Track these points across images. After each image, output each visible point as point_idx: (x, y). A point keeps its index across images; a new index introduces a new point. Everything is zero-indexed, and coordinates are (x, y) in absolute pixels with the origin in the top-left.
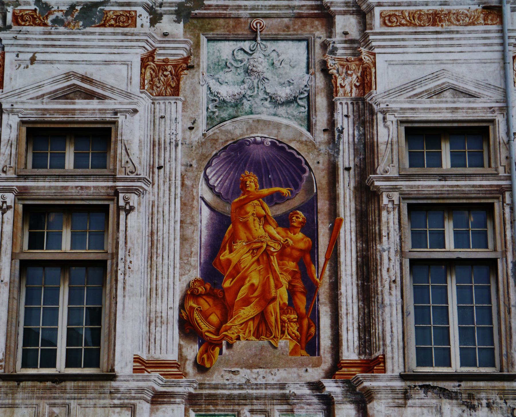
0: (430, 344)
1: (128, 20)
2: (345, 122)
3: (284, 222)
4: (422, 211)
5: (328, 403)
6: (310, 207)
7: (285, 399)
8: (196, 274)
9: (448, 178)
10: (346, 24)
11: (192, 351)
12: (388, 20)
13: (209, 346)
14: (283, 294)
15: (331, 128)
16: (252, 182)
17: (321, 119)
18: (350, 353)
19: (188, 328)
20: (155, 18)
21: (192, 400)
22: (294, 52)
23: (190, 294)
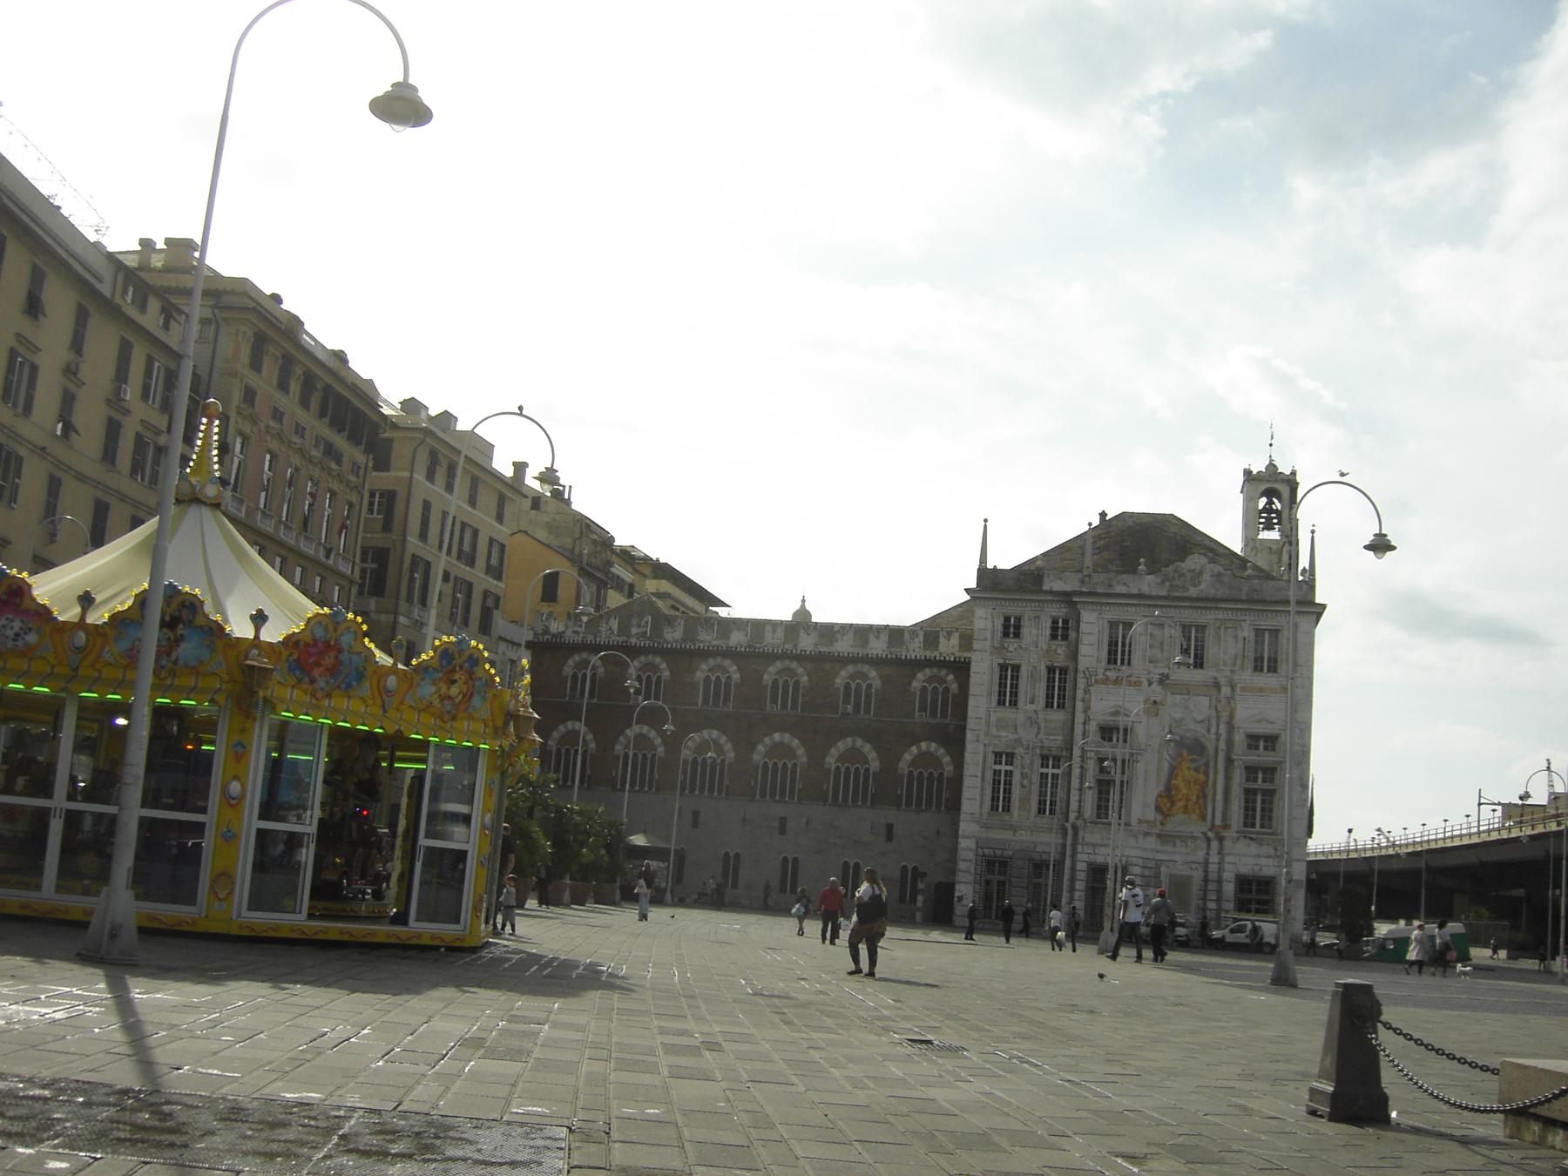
0: (1249, 821)
1: (1138, 684)
2: (1223, 730)
3: (1196, 770)
4: (1251, 771)
5: (1208, 840)
6: (1207, 765)
7: (1193, 838)
8: (1162, 788)
9: (1262, 757)
10: (1226, 690)
11: (1159, 817)
12: (1243, 689)
13: (1166, 816)
14: (1194, 798)
15: (1217, 734)
16: (1185, 753)
17: (1213, 730)
18: (1218, 822)
19: (1158, 808)
20: (1150, 684)
21: (1159, 836)
22: (1205, 701)
23: (1160, 796)
